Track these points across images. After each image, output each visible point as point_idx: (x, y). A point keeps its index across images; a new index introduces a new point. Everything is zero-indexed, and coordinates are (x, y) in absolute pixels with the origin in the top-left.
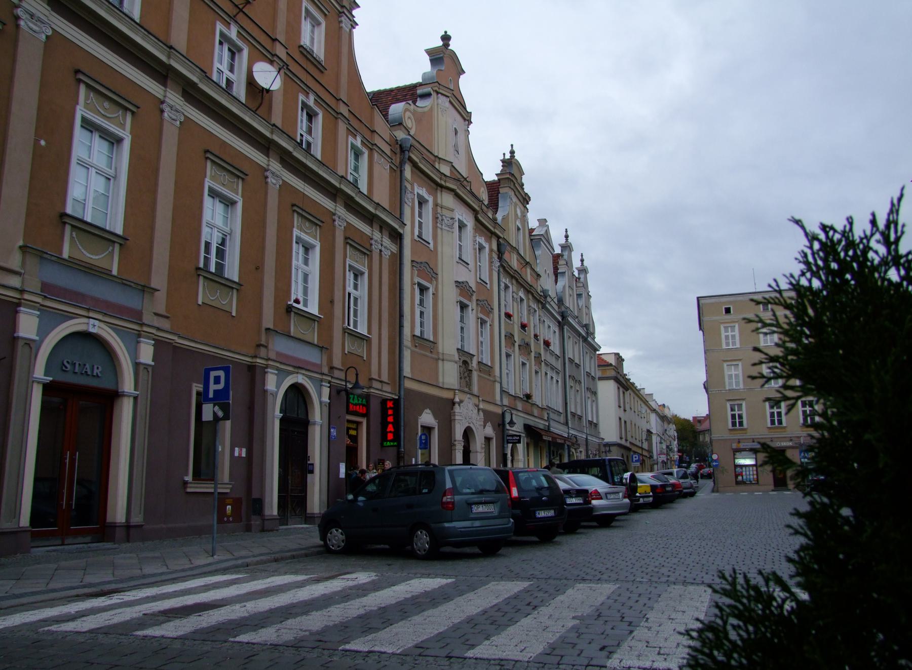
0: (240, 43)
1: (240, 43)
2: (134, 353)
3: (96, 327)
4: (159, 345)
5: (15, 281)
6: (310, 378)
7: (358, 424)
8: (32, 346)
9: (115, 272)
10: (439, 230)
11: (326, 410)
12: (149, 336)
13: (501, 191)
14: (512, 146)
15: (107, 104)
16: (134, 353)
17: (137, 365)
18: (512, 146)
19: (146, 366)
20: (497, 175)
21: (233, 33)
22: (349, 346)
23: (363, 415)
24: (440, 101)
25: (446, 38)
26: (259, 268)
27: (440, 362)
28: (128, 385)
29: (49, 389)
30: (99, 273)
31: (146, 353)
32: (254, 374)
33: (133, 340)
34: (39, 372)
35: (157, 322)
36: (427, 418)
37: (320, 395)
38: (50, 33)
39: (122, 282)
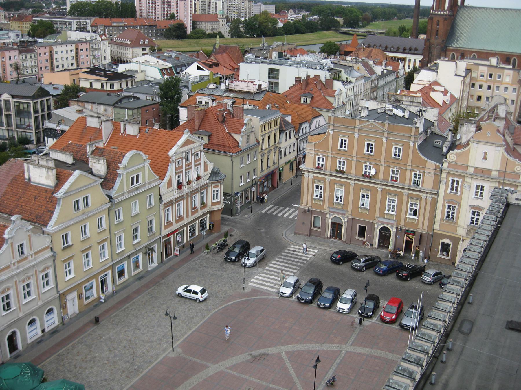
2: (344, 220)
3: (337, 216)
5: (326, 211)
8: (329, 218)
11: (395, 233)
16: (344, 220)
26: (375, 206)
28: (343, 224)
29: (332, 223)
31: (346, 220)
32: (372, 224)
33: (344, 218)
34: (330, 221)
36: (446, 241)
37: (393, 230)
39: (343, 210)
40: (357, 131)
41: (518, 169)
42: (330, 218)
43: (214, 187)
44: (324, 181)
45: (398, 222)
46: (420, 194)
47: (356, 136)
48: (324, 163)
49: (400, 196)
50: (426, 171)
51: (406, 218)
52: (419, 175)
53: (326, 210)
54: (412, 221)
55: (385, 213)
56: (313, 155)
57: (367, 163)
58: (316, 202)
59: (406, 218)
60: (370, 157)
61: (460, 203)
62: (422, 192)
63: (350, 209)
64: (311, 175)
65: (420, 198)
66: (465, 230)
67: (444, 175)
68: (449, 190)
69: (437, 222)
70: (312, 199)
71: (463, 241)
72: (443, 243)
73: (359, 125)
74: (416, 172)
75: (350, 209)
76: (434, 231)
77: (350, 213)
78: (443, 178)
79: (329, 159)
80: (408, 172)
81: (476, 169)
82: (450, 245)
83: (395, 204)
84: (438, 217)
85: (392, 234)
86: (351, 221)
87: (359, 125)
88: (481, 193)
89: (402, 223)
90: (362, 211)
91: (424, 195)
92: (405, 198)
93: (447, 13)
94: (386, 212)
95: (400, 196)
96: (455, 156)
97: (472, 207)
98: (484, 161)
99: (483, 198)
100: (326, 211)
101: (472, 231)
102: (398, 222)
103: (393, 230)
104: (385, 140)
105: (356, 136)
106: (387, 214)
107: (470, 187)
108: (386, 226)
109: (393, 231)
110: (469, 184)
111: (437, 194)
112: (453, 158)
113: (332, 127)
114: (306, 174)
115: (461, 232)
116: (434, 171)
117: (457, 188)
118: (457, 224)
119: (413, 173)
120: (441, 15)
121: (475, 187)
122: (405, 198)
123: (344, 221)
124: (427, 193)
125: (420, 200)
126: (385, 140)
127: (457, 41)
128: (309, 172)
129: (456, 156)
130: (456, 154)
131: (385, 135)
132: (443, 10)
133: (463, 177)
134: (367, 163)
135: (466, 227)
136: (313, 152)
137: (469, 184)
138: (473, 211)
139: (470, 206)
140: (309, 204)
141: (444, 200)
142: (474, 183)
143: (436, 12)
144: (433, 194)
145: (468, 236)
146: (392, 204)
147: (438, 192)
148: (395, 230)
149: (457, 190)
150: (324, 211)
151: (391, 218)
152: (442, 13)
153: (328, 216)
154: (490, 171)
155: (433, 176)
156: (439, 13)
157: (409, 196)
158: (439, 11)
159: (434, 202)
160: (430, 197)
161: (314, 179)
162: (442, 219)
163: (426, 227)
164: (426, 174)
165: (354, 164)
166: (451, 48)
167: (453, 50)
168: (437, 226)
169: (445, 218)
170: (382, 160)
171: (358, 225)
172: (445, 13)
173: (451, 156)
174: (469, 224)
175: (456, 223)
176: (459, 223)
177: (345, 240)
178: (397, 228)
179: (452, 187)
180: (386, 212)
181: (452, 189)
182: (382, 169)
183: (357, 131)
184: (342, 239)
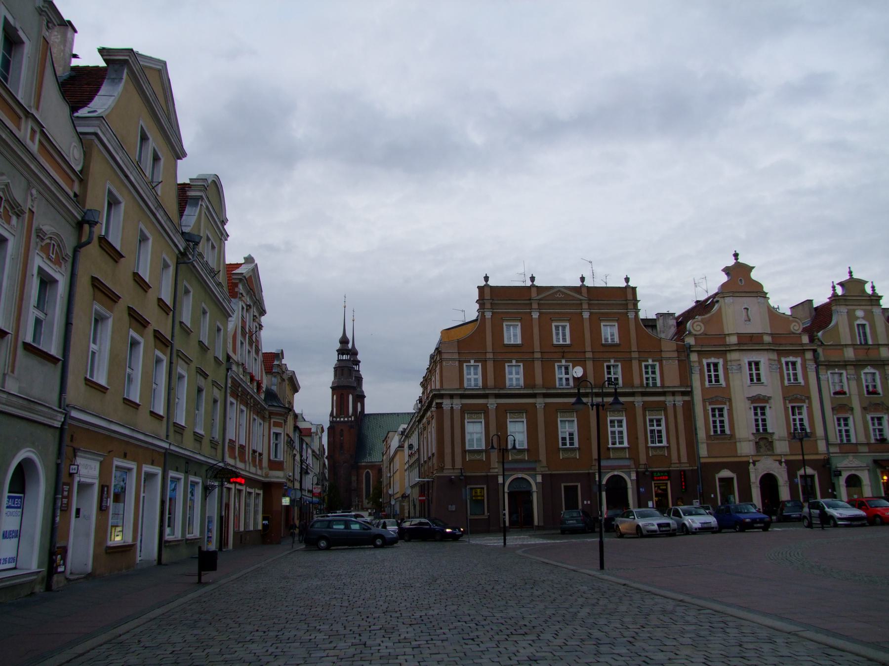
0: (567, 364)
1: (567, 364)
2: (535, 480)
3: (520, 476)
4: (544, 476)
5: (496, 470)
6: (622, 472)
7: (667, 484)
8: (504, 484)
9: (526, 459)
10: (730, 375)
11: (635, 482)
12: (539, 474)
13: (833, 308)
14: (850, 268)
15: (516, 414)
16: (535, 480)
17: (536, 483)
18: (850, 268)
19: (539, 483)
20: (829, 298)
21: (564, 362)
22: (652, 453)
23: (668, 480)
24: (726, 301)
25: (736, 255)
26: (589, 439)
27: (738, 444)
28: (534, 488)
30: (522, 461)
31: (539, 479)
34: (506, 490)
35: (542, 469)
36: (726, 473)
37: (630, 477)
38: (496, 405)
39: (528, 462)
40: (535, 306)
41: (796, 328)
42: (506, 483)
43: (276, 424)
44: (484, 410)
45: (634, 458)
46: (661, 398)
47: (535, 315)
48: (480, 376)
49: (629, 410)
50: (664, 355)
51: (647, 448)
52: (653, 367)
53: (496, 468)
54: (659, 452)
55: (608, 449)
56: (457, 363)
57: (561, 361)
58: (473, 458)
59: (647, 448)
60: (566, 350)
61: (730, 400)
62: (664, 394)
63: (543, 457)
64: (457, 403)
65: (662, 407)
66: (751, 442)
67: (694, 357)
68: (707, 383)
69: (702, 443)
70: (464, 451)
71: (754, 463)
72: (721, 480)
73: (538, 295)
74: (647, 361)
75: (543, 457)
76: (702, 460)
77: (544, 464)
78: (694, 362)
79: (490, 365)
80: (635, 364)
81: (739, 335)
82: (732, 479)
83: (624, 429)
84: (701, 434)
85: (629, 485)
86: (550, 481)
87: (538, 295)
88: (758, 375)
89: (643, 459)
90: (566, 456)
91: (669, 399)
92: (639, 411)
93: (353, 419)
94: (610, 446)
95: (629, 410)
96: (702, 325)
97: (753, 399)
98: (748, 323)
99: (762, 381)
100: (496, 470)
101: (762, 443)
102: (634, 458)
103: (630, 477)
104: (586, 315)
105: (535, 315)
106: (613, 449)
107: (740, 368)
108: (616, 473)
109: (630, 479)
110: (738, 362)
111: (689, 393)
112: (699, 328)
113: (488, 306)
114: (446, 403)
115: (746, 449)
116: (675, 355)
117: (717, 376)
118: (735, 438)
119: (643, 364)
120: (344, 422)
121: (747, 365)
122: (639, 411)
123: (535, 482)
124: (673, 394)
125: (665, 409)
126: (586, 315)
127: (370, 454)
128: (452, 396)
129: (703, 324)
130: (702, 321)
131: (585, 306)
132: (347, 416)
133: (723, 353)
134: (561, 361)
135: (752, 438)
136: (456, 356)
137: (738, 362)
138: (755, 408)
139: (749, 398)
140: (459, 465)
141: (704, 401)
142: (746, 358)
143: (338, 419)
144: (684, 393)
145: (760, 454)
146: (616, 429)
147: (691, 387)
148: (634, 476)
149: (717, 381)
150: (494, 472)
151: (622, 455)
152: (346, 419)
153: (500, 480)
154: (760, 335)
155: (677, 362)
156: (342, 419)
157: (646, 407)
158: (342, 417)
159: (689, 408)
160: (679, 400)
161: (465, 410)
162: (709, 437)
163: (684, 459)
164: (664, 362)
165: (538, 366)
166: (363, 464)
167: (366, 467)
168: (703, 451)
169: (712, 433)
170: (587, 350)
171: (563, 485)
172: (350, 419)
173: (695, 325)
174: (755, 432)
175: (732, 436)
176: (737, 436)
177: (542, 524)
178: (637, 473)
179: (710, 376)
180: (610, 446)
181: (710, 381)
182: (590, 365)
183: (535, 306)
184: (536, 523)
